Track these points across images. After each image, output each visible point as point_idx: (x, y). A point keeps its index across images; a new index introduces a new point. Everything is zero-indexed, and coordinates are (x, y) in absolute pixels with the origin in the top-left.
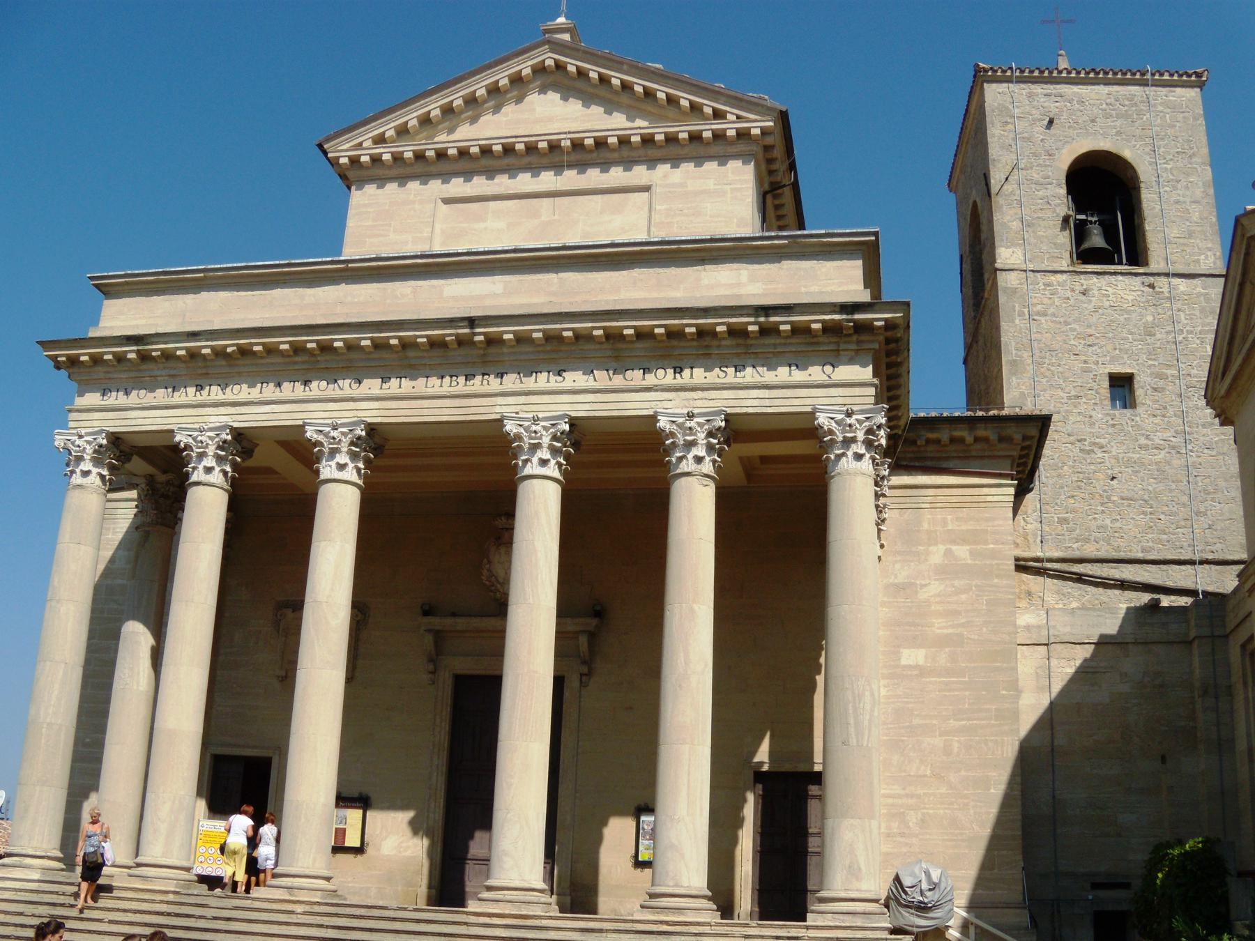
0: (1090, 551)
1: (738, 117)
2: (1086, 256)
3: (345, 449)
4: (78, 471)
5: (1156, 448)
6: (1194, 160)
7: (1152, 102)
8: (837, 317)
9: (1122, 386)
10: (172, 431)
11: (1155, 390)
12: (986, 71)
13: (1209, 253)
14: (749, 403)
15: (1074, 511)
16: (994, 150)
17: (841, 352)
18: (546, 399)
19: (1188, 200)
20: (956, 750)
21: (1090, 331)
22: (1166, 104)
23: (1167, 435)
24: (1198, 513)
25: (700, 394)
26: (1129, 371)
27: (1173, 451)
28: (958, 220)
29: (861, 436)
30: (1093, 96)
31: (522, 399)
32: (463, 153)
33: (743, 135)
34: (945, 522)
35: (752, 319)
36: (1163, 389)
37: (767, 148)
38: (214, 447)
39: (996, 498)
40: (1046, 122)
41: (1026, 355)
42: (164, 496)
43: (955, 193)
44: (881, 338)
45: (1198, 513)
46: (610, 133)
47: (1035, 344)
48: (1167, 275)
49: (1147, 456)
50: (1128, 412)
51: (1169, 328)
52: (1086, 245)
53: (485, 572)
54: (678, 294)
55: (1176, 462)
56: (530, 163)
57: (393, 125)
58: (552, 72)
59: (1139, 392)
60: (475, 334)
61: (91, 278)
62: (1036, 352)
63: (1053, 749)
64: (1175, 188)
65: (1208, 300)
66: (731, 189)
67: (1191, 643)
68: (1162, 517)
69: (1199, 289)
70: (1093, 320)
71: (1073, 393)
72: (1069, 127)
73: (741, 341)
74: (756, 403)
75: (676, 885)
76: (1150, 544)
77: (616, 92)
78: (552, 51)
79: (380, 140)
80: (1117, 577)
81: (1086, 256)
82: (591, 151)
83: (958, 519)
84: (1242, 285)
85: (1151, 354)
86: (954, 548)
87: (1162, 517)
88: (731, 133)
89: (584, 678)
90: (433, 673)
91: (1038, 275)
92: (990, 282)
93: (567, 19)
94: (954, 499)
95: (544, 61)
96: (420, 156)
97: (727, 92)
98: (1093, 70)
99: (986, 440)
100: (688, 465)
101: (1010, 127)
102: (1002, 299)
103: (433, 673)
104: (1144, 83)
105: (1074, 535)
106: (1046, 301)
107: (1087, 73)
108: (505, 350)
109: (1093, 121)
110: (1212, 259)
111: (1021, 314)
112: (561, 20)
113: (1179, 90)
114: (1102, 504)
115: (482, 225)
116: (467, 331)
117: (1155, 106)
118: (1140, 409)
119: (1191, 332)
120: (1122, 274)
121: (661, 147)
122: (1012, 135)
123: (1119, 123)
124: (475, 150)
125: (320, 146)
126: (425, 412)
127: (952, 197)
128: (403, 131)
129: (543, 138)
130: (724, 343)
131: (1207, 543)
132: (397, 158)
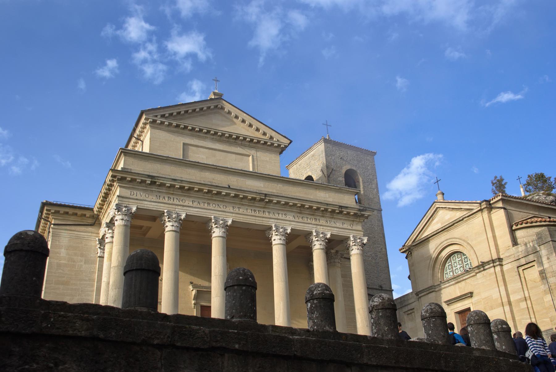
5: (369, 257)
8: (357, 212)
17: (354, 221)
18: (283, 222)
23: (371, 253)
27: (373, 258)
46: (241, 136)
51: (370, 223)
56: (213, 138)
60: (266, 199)
66: (274, 162)
68: (371, 276)
76: (369, 283)
79: (163, 116)
95: (218, 105)
96: (178, 126)
115: (198, 156)
116: (264, 197)
119: (375, 225)
126: (248, 220)
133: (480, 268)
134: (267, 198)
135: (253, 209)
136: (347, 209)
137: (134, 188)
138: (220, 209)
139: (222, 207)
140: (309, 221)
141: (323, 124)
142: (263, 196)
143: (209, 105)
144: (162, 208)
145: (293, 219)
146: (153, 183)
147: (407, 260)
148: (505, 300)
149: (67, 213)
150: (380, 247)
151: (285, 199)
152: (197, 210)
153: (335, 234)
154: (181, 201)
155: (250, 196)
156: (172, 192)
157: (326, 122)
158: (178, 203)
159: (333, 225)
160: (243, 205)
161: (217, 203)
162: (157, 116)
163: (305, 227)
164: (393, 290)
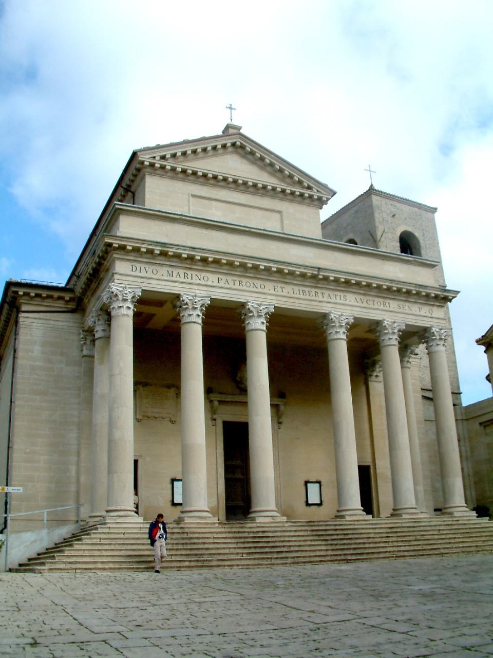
1: (317, 191)
3: (264, 316)
8: (439, 293)
16: (377, 224)
31: (333, 306)
32: (184, 171)
33: (320, 199)
35: (414, 289)
74: (412, 321)
78: (240, 138)
89: (280, 425)
101: (381, 215)
116: (316, 273)
129: (240, 178)
134: (321, 273)
135: (301, 289)
136: (426, 289)
137: (172, 266)
138: (255, 290)
139: (259, 287)
140: (376, 306)
141: (365, 170)
143: (225, 142)
144: (176, 289)
145: (356, 304)
146: (164, 254)
149: (37, 295)
151: (345, 275)
152: (224, 291)
154: (202, 279)
155: (298, 271)
156: (189, 266)
157: (368, 167)
158: (198, 282)
159: (408, 311)
160: (286, 283)
161: (251, 281)
162: (155, 158)
163: (371, 315)
164: (461, 393)
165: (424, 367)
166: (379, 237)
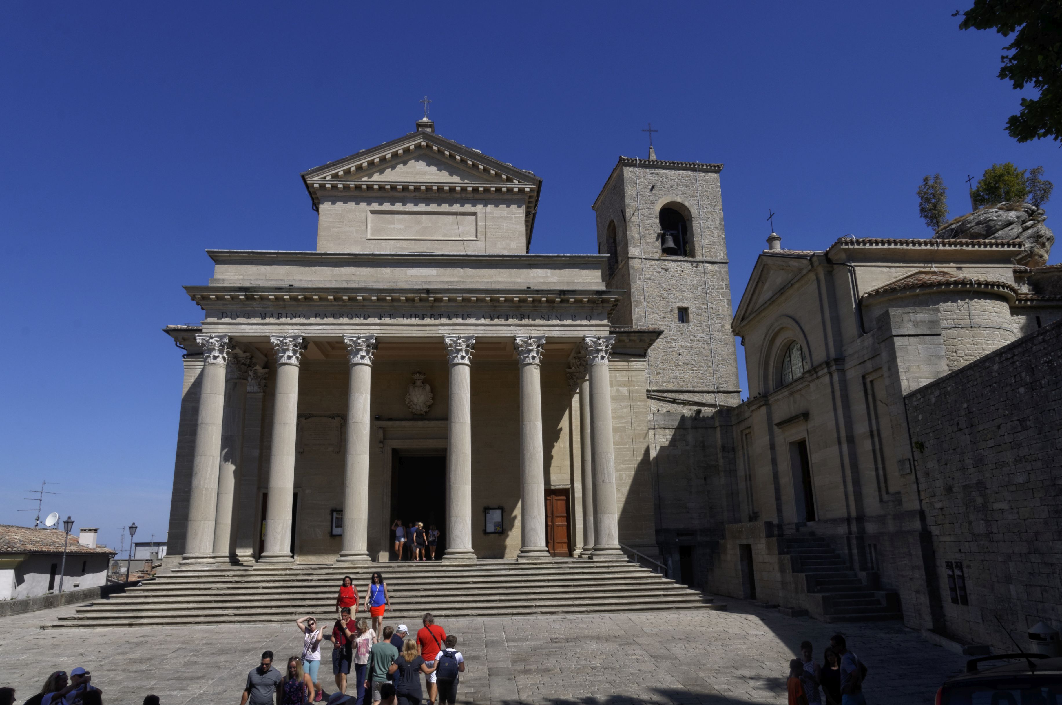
0: (670, 387)
2: (667, 251)
4: (211, 356)
6: (716, 208)
7: (698, 179)
9: (683, 314)
10: (269, 337)
11: (697, 315)
12: (624, 160)
13: (721, 252)
14: (555, 332)
15: (663, 369)
16: (628, 200)
18: (463, 328)
19: (712, 227)
20: (624, 478)
21: (670, 287)
22: (705, 181)
23: (703, 335)
24: (716, 370)
25: (533, 328)
26: (686, 306)
28: (598, 226)
29: (604, 348)
30: (672, 175)
31: (451, 328)
33: (521, 191)
34: (616, 377)
36: (701, 315)
37: (530, 197)
38: (292, 346)
39: (638, 367)
40: (650, 187)
41: (642, 297)
42: (243, 364)
43: (596, 211)
44: (611, 305)
45: (716, 370)
47: (645, 293)
48: (703, 262)
49: (694, 345)
50: (685, 325)
51: (704, 286)
52: (666, 246)
53: (407, 400)
54: (519, 280)
55: (706, 347)
56: (415, 196)
57: (342, 169)
58: (424, 148)
59: (691, 317)
61: (208, 252)
62: (646, 297)
63: (658, 475)
64: (707, 221)
65: (720, 274)
67: (716, 428)
68: (701, 372)
69: (717, 269)
70: (671, 282)
71: (662, 315)
72: (662, 190)
73: (551, 305)
74: (558, 332)
75: (535, 546)
77: (457, 163)
80: (682, 398)
81: (667, 251)
82: (447, 193)
83: (622, 376)
84: (758, 283)
85: (695, 299)
86: (620, 388)
87: (701, 372)
88: (516, 189)
90: (382, 448)
91: (647, 261)
92: (623, 263)
93: (429, 119)
94: (620, 367)
96: (358, 187)
97: (513, 169)
98: (673, 163)
99: (634, 341)
100: (529, 360)
101: (635, 188)
102: (631, 272)
103: (382, 448)
104: (694, 170)
105: (663, 380)
106: (650, 273)
107: (670, 164)
108: (442, 304)
109: (672, 187)
110: (722, 255)
111: (640, 279)
112: (425, 119)
113: (710, 174)
114: (675, 366)
115: (392, 226)
117: (699, 181)
118: (691, 324)
120: (684, 261)
121: (481, 193)
122: (635, 193)
123: (683, 188)
124: (388, 187)
125: (303, 177)
127: (594, 212)
128: (347, 172)
130: (543, 305)
131: (720, 384)
132: (346, 188)
133: (813, 375)
141: (643, 131)
142: (424, 293)
144: (268, 331)
147: (743, 347)
148: (843, 434)
150: (720, 323)
153: (556, 336)
165: (684, 364)
166: (628, 215)
